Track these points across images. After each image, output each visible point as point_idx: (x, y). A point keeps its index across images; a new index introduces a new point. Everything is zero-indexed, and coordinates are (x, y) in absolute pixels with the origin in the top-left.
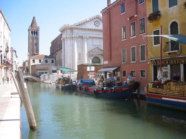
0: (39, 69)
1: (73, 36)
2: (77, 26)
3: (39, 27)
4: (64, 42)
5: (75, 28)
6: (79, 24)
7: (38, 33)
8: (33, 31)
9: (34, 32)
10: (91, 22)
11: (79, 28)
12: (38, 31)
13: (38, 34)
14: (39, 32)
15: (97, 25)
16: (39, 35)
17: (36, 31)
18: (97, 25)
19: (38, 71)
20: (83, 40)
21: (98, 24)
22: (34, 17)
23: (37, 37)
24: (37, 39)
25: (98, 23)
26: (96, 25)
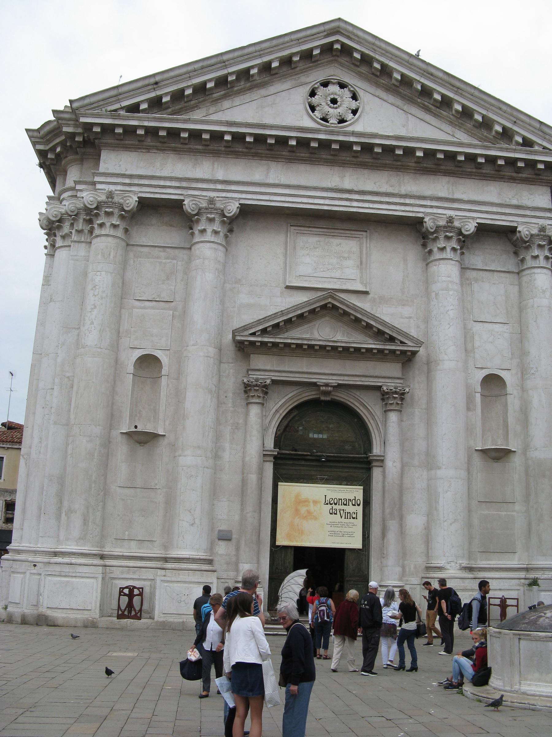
2: (134, 109)
5: (107, 129)
6: (156, 104)
11: (152, 132)
15: (333, 113)
18: (333, 113)
21: (346, 103)
26: (326, 108)
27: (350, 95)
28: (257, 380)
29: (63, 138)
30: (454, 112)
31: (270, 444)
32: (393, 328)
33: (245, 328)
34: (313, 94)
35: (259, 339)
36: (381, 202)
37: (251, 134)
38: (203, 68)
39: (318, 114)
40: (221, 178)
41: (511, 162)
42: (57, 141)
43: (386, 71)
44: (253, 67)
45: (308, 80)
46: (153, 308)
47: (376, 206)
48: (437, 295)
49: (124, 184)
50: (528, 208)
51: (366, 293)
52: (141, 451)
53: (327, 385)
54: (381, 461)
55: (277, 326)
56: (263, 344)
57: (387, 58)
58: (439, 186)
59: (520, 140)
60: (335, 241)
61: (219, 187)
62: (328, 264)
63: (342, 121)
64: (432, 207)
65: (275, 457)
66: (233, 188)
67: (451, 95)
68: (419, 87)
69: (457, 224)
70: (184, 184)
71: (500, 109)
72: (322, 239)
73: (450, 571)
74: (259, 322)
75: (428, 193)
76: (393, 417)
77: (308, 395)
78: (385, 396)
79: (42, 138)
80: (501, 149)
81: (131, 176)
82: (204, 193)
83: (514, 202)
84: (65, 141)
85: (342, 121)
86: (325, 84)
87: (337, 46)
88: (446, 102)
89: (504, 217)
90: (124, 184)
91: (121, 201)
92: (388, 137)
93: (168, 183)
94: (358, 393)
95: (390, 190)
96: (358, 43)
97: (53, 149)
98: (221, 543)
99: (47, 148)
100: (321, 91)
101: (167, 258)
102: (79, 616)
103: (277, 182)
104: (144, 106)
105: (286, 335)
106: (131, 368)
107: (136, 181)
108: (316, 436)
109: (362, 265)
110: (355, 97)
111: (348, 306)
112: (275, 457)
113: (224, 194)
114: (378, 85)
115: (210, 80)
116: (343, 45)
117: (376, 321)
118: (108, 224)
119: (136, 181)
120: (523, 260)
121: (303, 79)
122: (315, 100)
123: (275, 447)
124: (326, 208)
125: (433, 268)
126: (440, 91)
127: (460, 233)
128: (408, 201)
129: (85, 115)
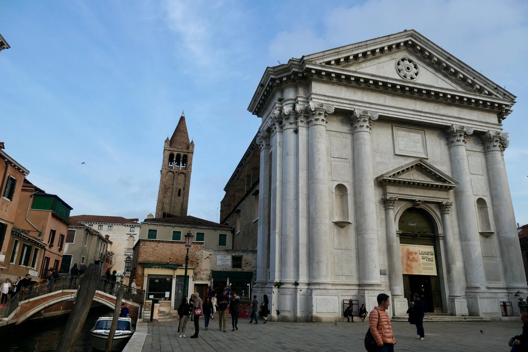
0: (152, 259)
1: (312, 105)
2: (329, 63)
3: (192, 142)
4: (269, 146)
5: (318, 72)
6: (338, 61)
7: (189, 159)
8: (175, 153)
9: (178, 156)
10: (383, 59)
11: (338, 76)
12: (189, 155)
13: (189, 162)
14: (191, 159)
15: (409, 74)
16: (191, 164)
17: (182, 154)
18: (409, 74)
19: (148, 271)
20: (353, 132)
22: (182, 119)
23: (184, 171)
24: (186, 175)
25: (411, 65)
27: (413, 66)
28: (392, 198)
29: (290, 73)
30: (458, 78)
31: (398, 229)
32: (446, 176)
33: (388, 173)
34: (398, 64)
35: (393, 179)
36: (433, 118)
37: (381, 81)
38: (358, 47)
39: (402, 74)
40: (366, 101)
41: (485, 102)
42: (285, 74)
43: (431, 57)
44: (377, 49)
45: (396, 57)
46: (339, 161)
47: (431, 119)
48: (459, 161)
49: (325, 100)
50: (491, 124)
51: (427, 159)
52: (343, 231)
53: (419, 201)
54: (444, 238)
55: (398, 173)
56: (395, 181)
57: (432, 50)
58: (454, 111)
59: (487, 92)
60: (412, 134)
61: (367, 105)
62: (413, 145)
63: (412, 78)
64: (453, 121)
65: (400, 235)
66: (373, 106)
67: (459, 70)
68: (445, 65)
69: (465, 130)
70: (352, 103)
71: (480, 78)
72: (406, 133)
73: (483, 289)
74: (393, 171)
75: (450, 115)
76: (447, 217)
77: (409, 205)
78: (442, 207)
79: (275, 72)
80: (482, 96)
81: (328, 97)
82: (361, 108)
83: (484, 121)
84: (290, 75)
85: (412, 78)
86: (403, 60)
87: (410, 42)
88: (456, 73)
89: (481, 127)
90: (325, 100)
91: (326, 109)
92: (437, 88)
93: (345, 102)
94: (429, 205)
95: (435, 112)
96: (419, 42)
97: (281, 79)
98: (382, 276)
99: (277, 77)
100: (401, 63)
101: (343, 138)
102: (332, 316)
103: (389, 105)
104: (333, 62)
105: (400, 177)
106: (334, 191)
107: (331, 99)
108: (411, 225)
109: (425, 146)
110: (416, 67)
111: (427, 165)
112: (400, 235)
113: (369, 109)
114: (425, 62)
115: (360, 53)
116: (412, 42)
117: (439, 172)
118: (320, 119)
119: (331, 99)
120: (488, 147)
121: (394, 56)
122: (400, 67)
123: (399, 229)
124: (411, 119)
125: (454, 149)
126: (454, 68)
127: (465, 133)
128: (444, 118)
129: (309, 64)
